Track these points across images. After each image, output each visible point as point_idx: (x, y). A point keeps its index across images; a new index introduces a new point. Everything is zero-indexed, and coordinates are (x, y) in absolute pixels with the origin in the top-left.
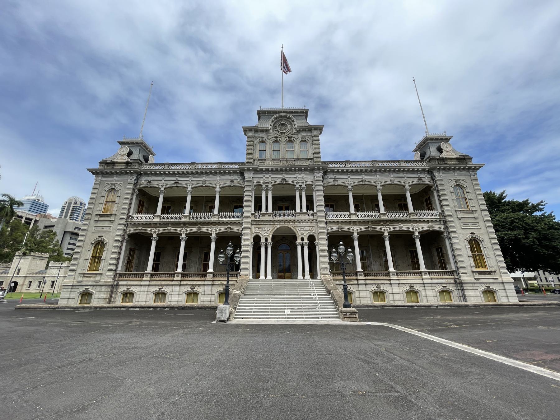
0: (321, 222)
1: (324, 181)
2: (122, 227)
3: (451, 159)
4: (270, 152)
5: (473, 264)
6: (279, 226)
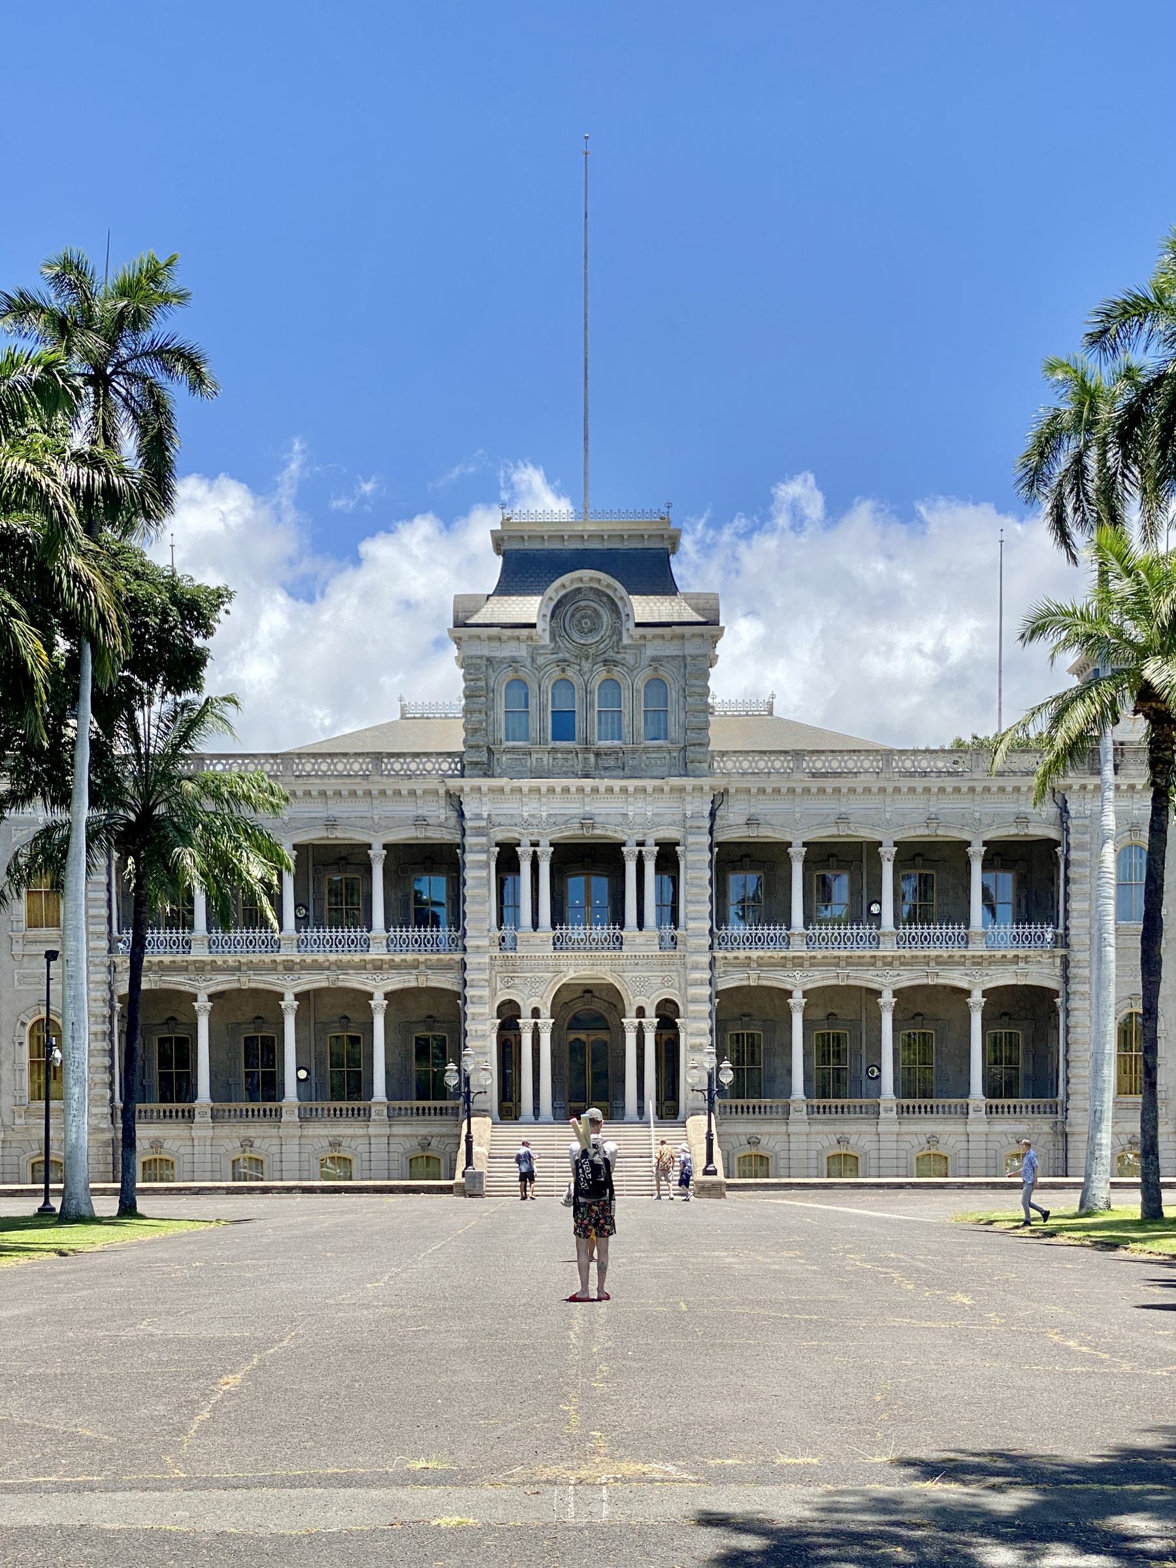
1: (718, 821)
4: (542, 721)
6: (571, 974)
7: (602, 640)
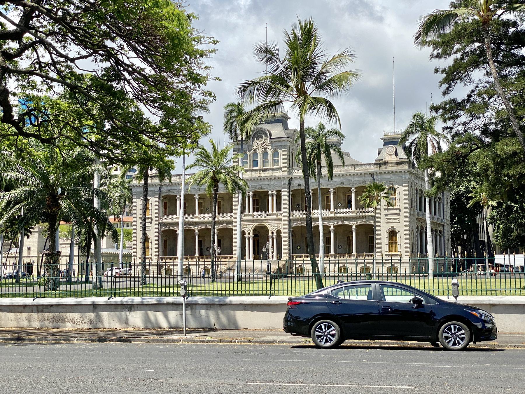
0: (284, 221)
1: (291, 185)
2: (157, 226)
3: (391, 163)
5: (387, 250)
6: (257, 224)
7: (264, 143)
